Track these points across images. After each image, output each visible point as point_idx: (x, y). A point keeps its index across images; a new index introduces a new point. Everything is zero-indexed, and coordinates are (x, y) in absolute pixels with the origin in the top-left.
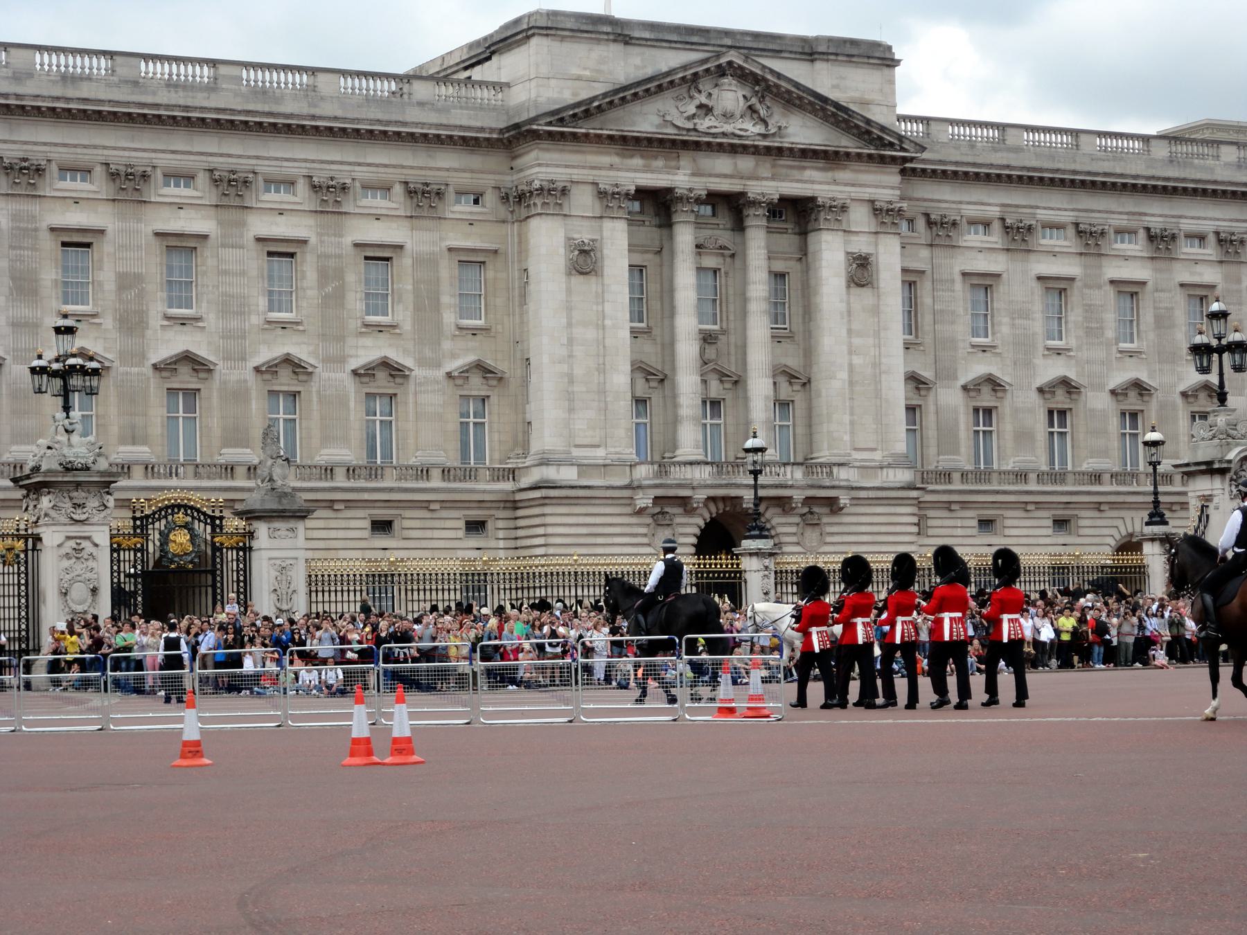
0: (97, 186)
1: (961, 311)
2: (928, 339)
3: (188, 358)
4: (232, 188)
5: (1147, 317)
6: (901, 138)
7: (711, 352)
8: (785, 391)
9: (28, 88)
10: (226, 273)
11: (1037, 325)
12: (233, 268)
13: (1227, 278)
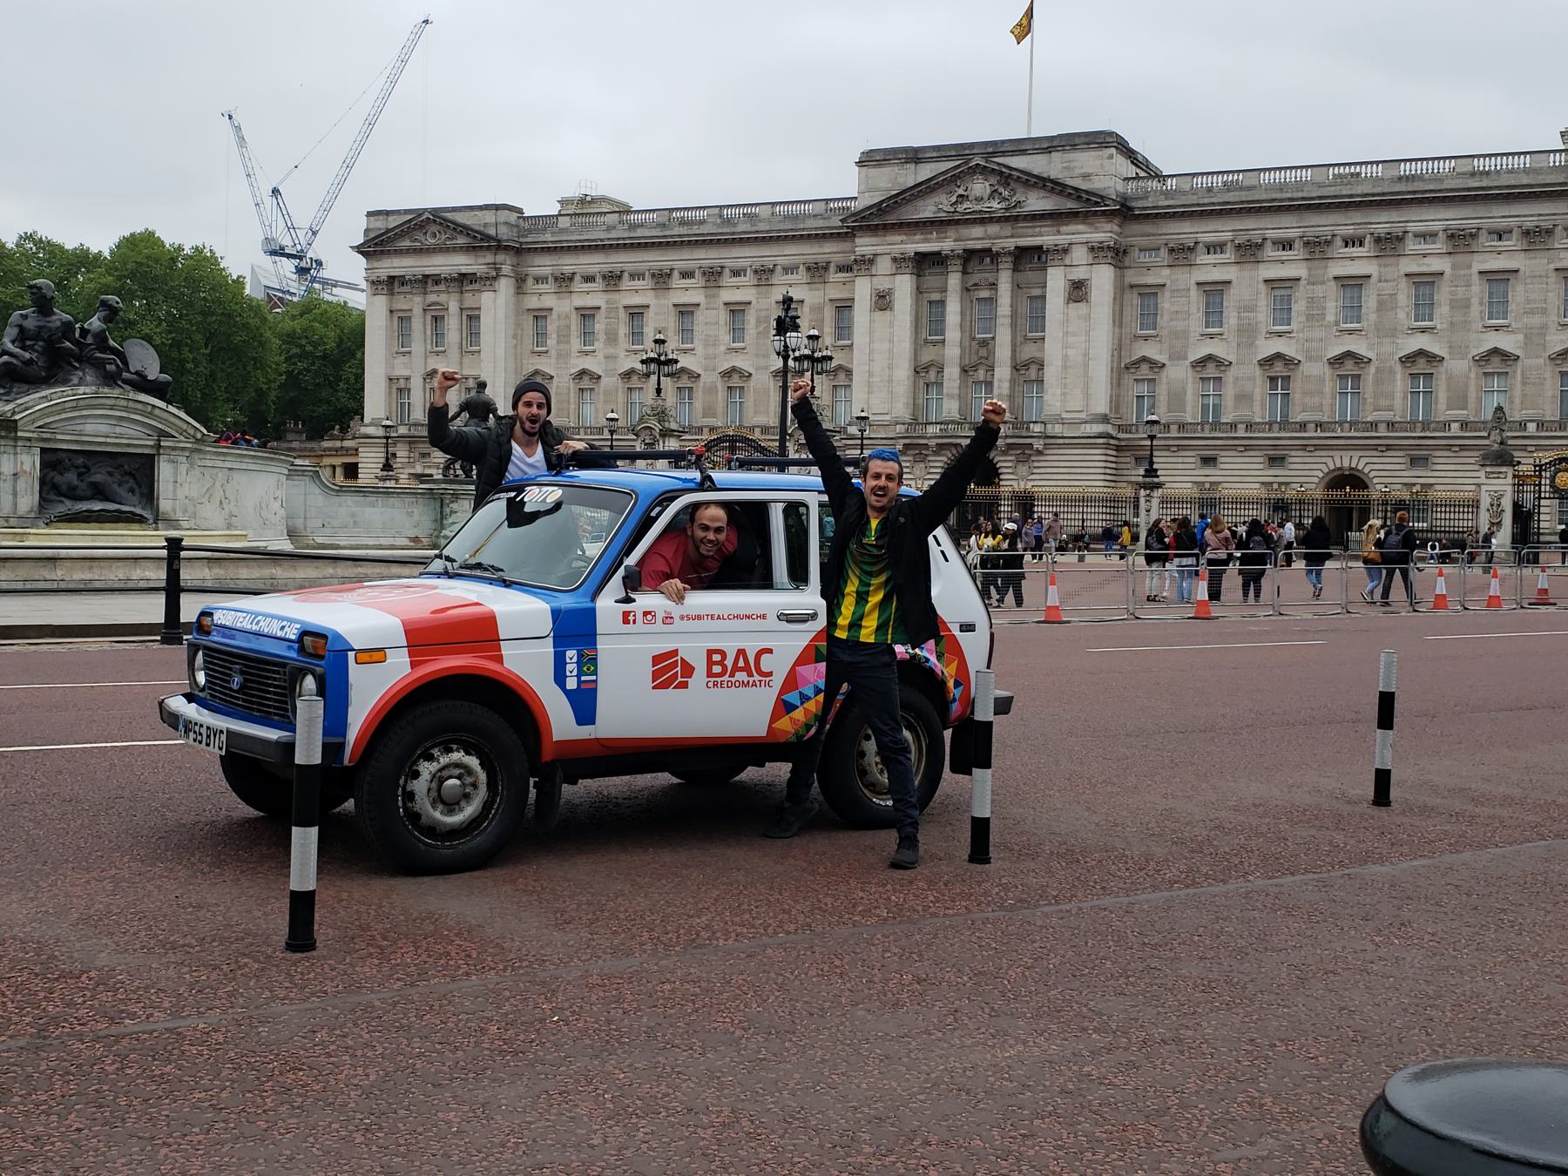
0: (647, 283)
1: (1193, 309)
2: (1165, 332)
6: (1101, 197)
7: (983, 352)
9: (613, 235)
11: (1263, 316)
12: (711, 321)
13: (1454, 267)
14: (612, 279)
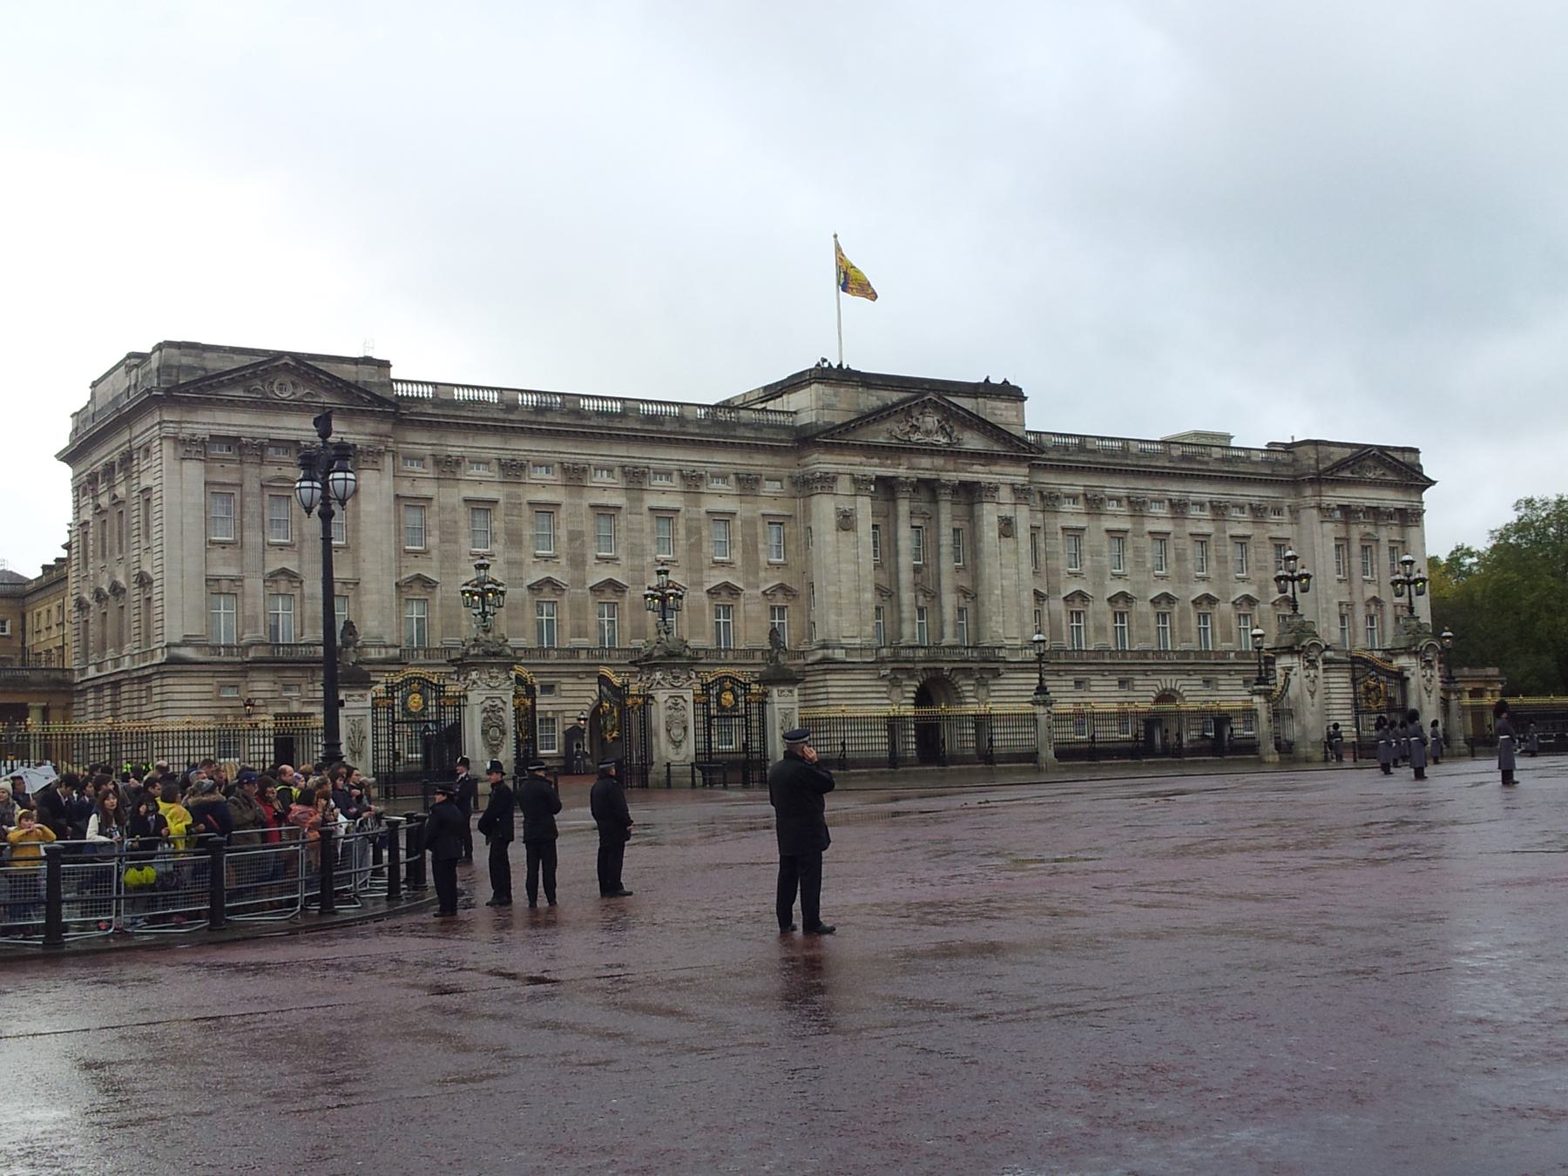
0: (556, 477)
2: (1043, 568)
3: (610, 583)
4: (635, 478)
5: (1171, 554)
7: (919, 577)
8: (962, 600)
10: (630, 530)
11: (1106, 561)
13: (1217, 530)
14: (512, 470)
